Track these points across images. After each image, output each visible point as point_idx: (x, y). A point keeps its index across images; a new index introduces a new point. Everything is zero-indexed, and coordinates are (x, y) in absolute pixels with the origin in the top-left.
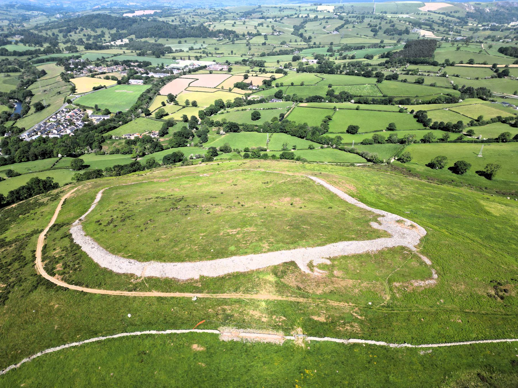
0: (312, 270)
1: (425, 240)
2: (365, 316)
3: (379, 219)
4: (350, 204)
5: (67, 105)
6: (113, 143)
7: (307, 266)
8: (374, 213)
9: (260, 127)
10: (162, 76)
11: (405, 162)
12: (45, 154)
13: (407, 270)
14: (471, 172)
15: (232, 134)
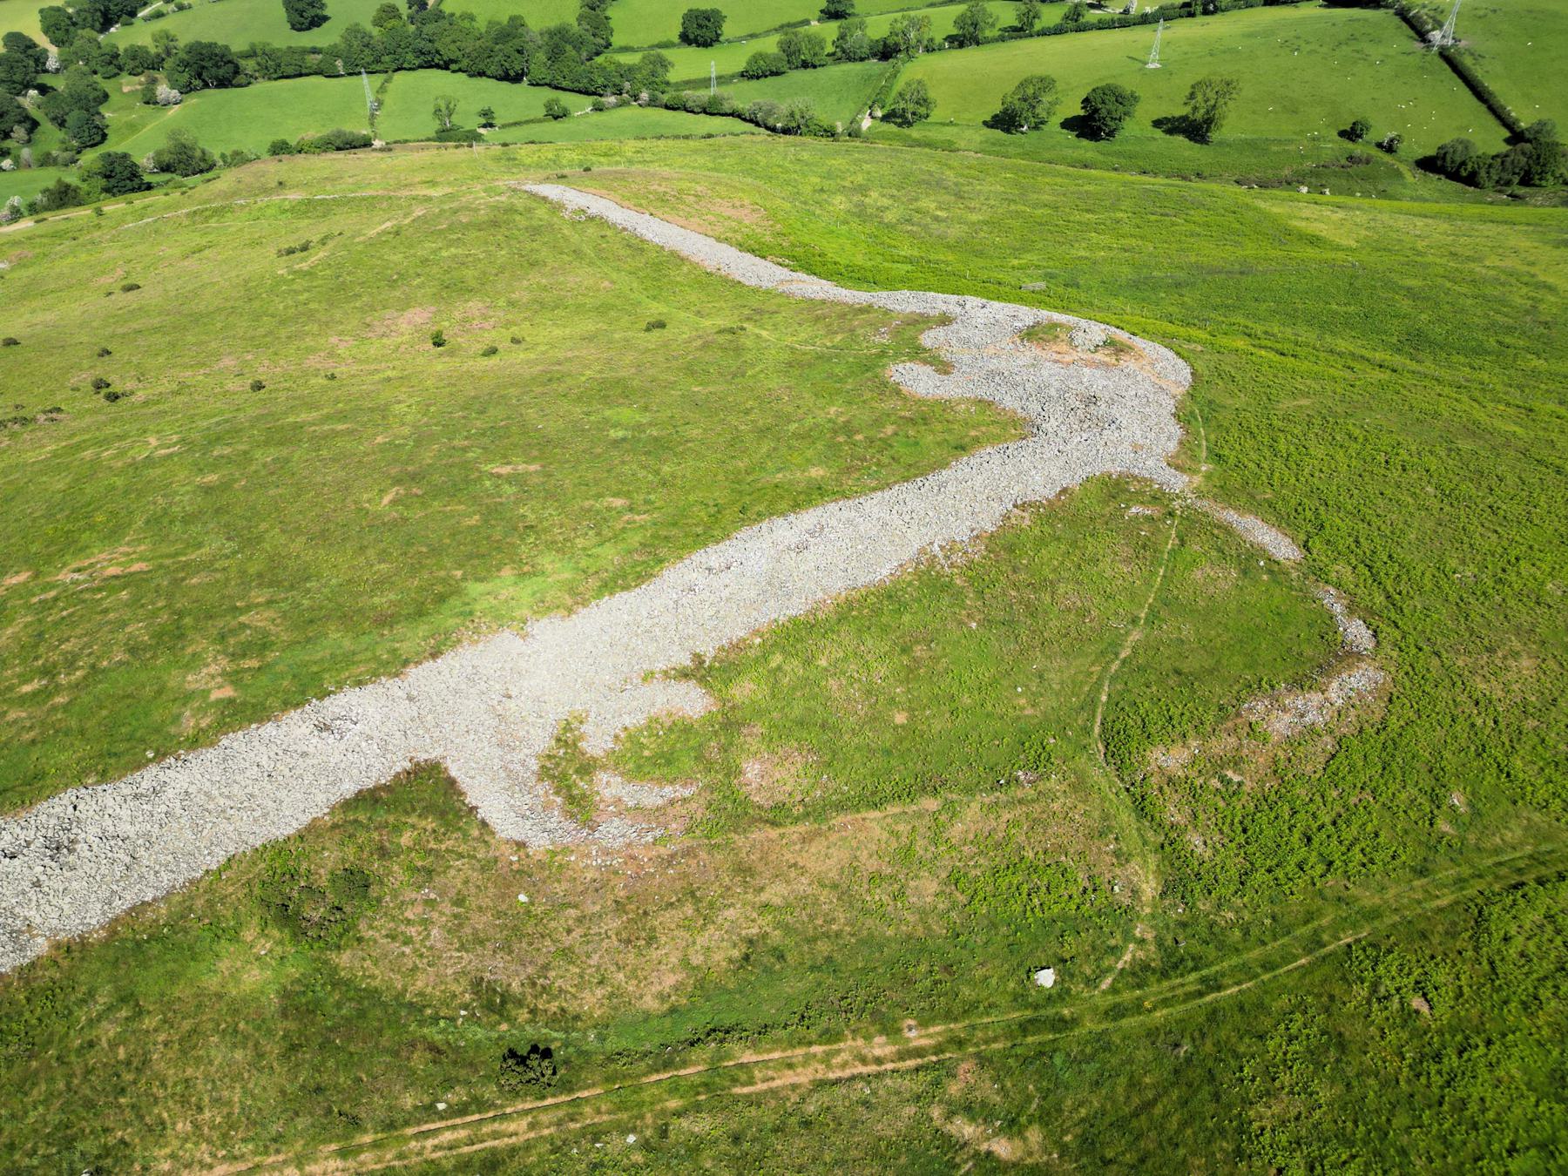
0: (579, 806)
1: (1196, 411)
2: (1044, 1118)
3: (928, 339)
4: (755, 291)
7: (544, 773)
8: (887, 312)
9: (333, 53)
11: (910, 124)
13: (1188, 631)
14: (1136, 127)
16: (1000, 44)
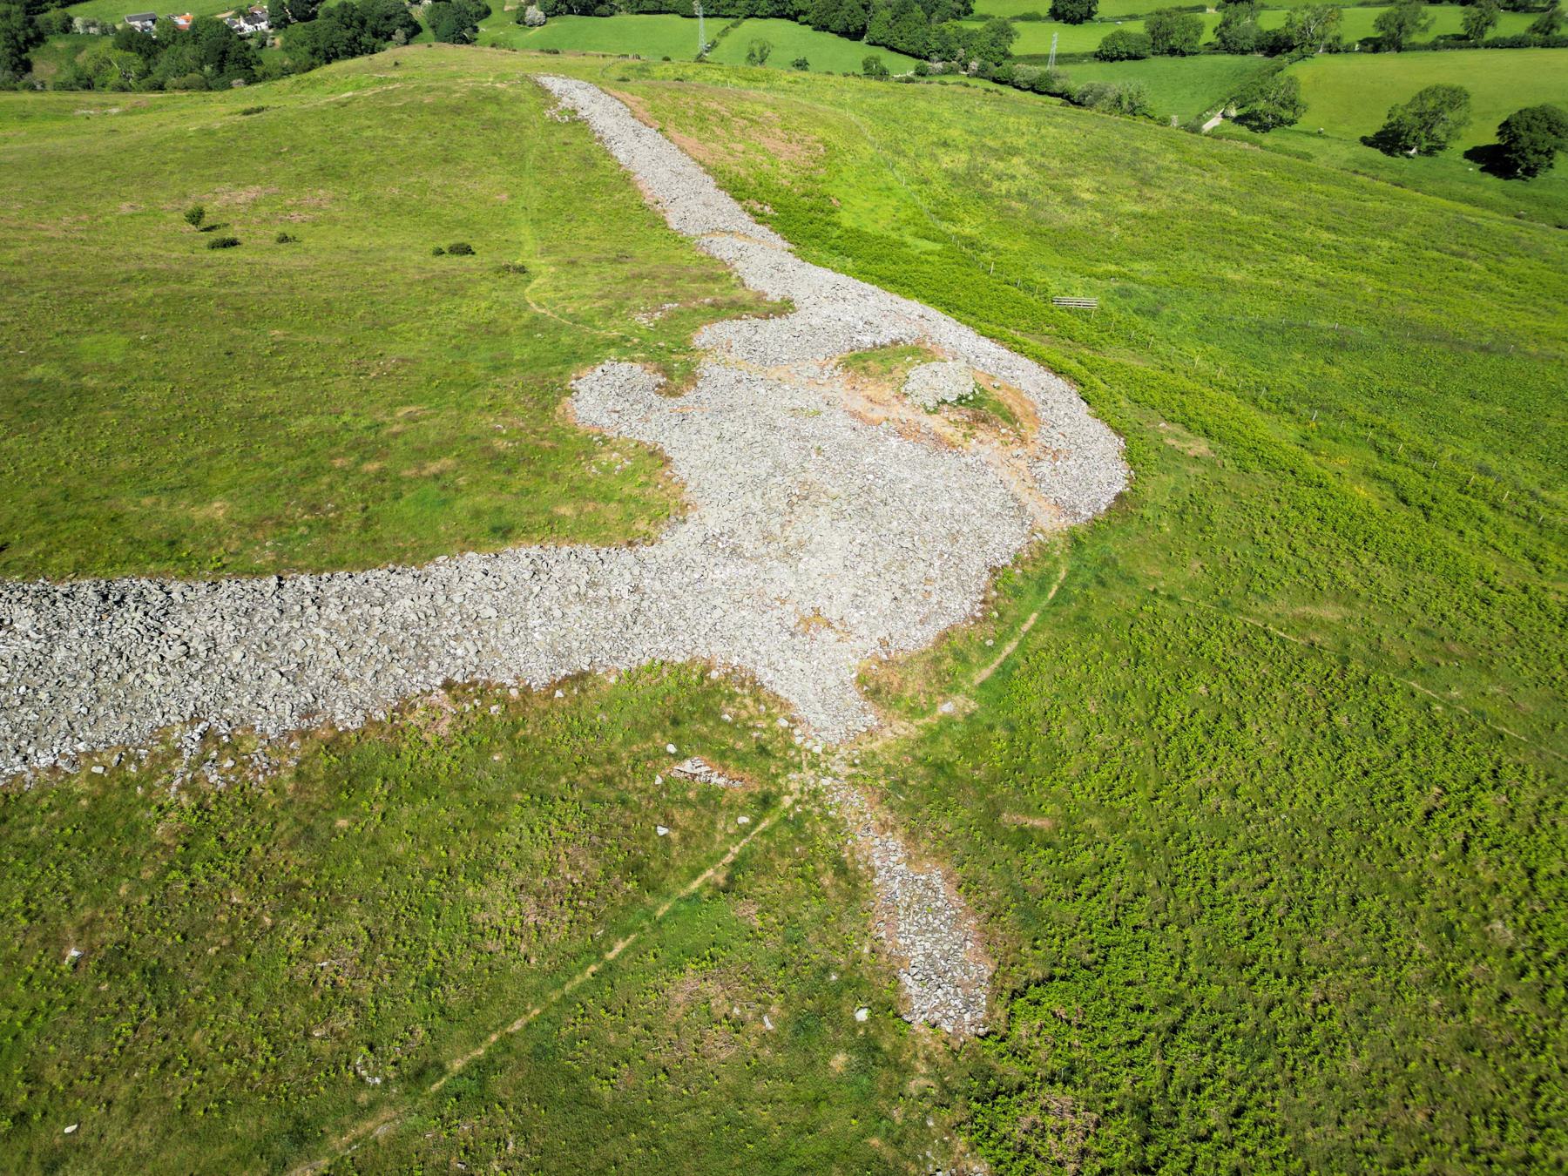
6: (78, 49)
11: (1266, 128)
15: (574, 20)
16: (1432, 54)
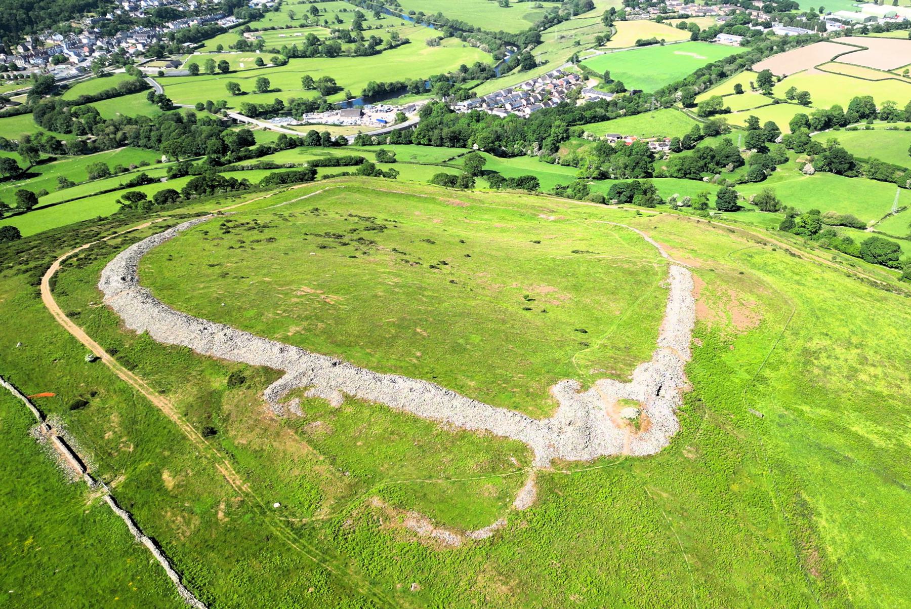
5: (570, 64)
10: (793, 32)
12: (457, 140)
